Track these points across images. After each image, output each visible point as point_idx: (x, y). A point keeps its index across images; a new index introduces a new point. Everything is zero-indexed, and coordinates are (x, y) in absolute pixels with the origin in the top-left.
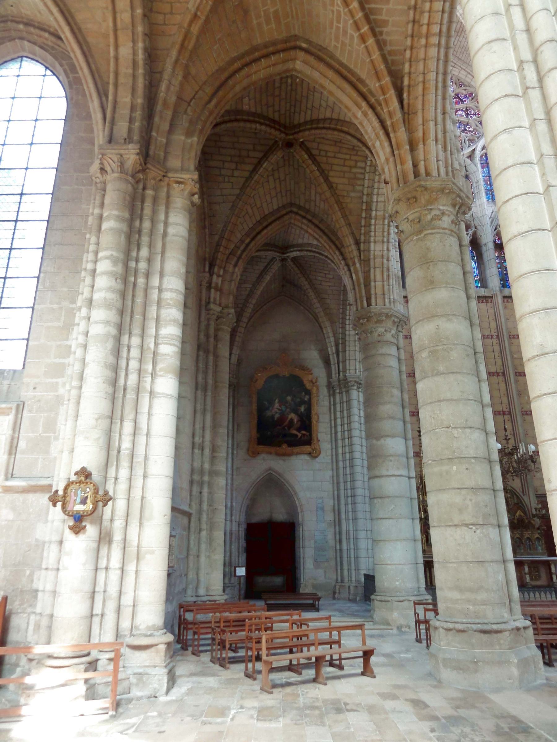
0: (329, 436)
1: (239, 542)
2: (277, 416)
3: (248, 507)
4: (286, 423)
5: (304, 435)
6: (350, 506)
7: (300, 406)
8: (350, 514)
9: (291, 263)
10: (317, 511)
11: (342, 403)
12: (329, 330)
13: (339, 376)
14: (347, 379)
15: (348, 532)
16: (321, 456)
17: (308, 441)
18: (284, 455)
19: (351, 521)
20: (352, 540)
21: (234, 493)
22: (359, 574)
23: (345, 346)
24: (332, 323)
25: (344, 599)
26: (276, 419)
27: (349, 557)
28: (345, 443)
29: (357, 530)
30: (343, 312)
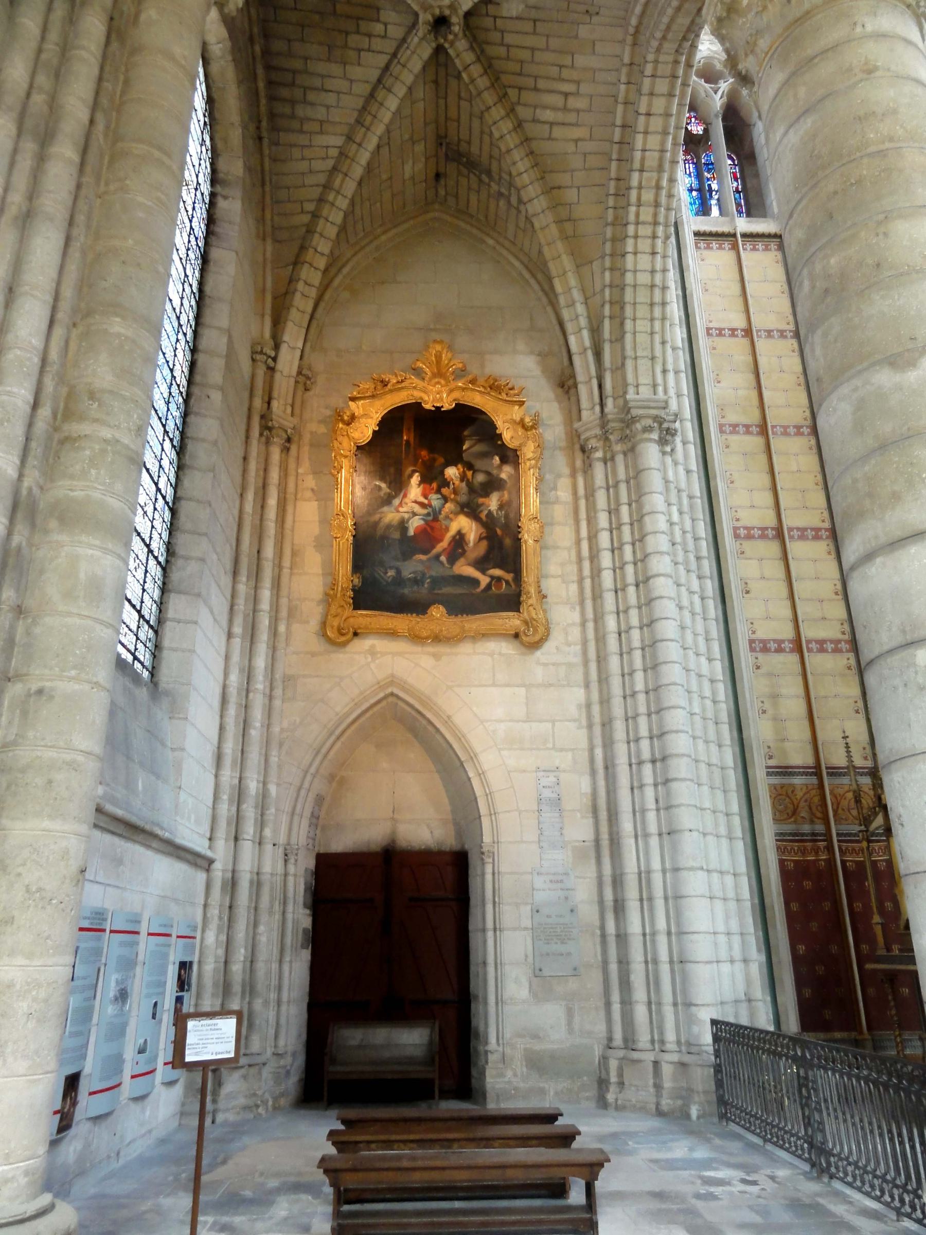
0: (574, 587)
1: (284, 913)
2: (415, 524)
3: (319, 800)
4: (444, 544)
5: (499, 579)
6: (650, 793)
7: (487, 495)
8: (651, 816)
9: (462, 44)
10: (540, 811)
11: (611, 487)
12: (573, 281)
13: (602, 405)
14: (628, 412)
15: (644, 876)
16: (550, 646)
17: (512, 602)
18: (437, 639)
19: (654, 842)
20: (659, 904)
21: (274, 753)
22: (691, 1020)
23: (622, 324)
24: (581, 263)
25: (641, 1109)
26: (411, 532)
27: (652, 961)
28: (625, 599)
29: (676, 870)
30: (616, 218)
